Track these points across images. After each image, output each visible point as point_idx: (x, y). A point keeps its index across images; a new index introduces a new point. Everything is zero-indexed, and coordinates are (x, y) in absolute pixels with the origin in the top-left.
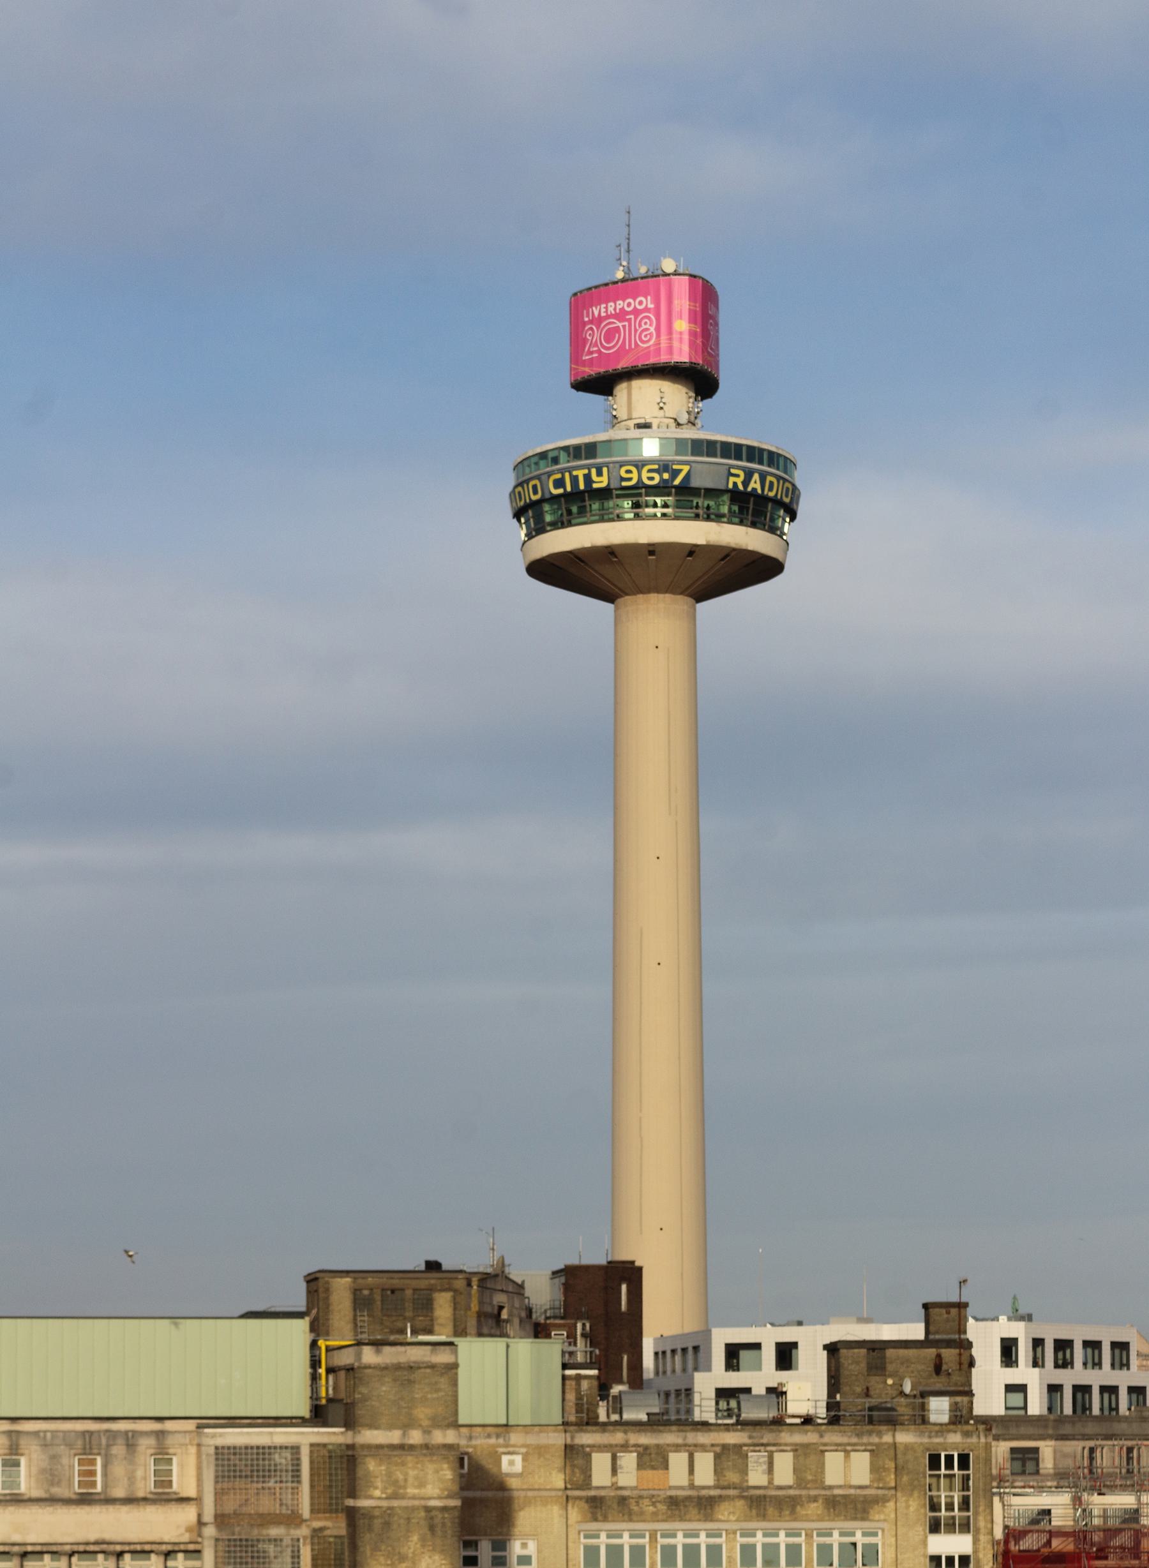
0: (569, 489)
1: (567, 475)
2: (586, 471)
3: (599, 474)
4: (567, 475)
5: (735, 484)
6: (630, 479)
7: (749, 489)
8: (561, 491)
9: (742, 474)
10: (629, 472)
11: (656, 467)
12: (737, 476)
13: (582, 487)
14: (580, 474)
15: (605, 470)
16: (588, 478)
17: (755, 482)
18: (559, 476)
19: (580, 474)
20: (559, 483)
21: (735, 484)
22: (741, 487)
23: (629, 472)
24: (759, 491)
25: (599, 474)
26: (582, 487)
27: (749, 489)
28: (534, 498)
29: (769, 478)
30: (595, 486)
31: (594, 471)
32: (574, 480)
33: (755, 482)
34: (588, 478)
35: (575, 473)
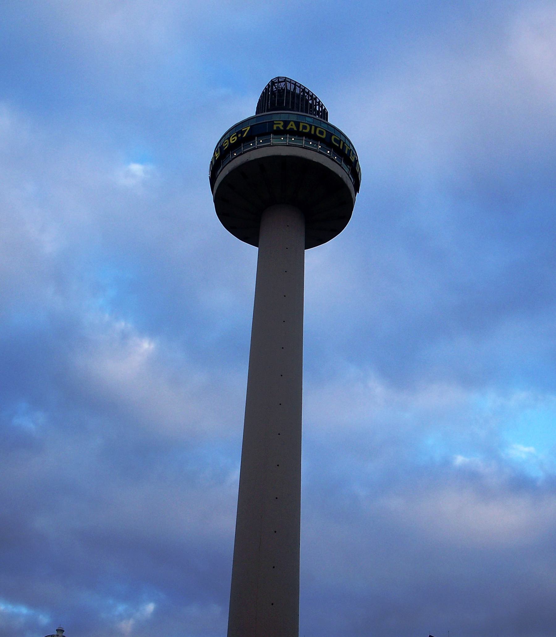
5: (277, 127)
7: (288, 128)
12: (280, 124)
17: (292, 125)
22: (282, 128)
24: (295, 129)
27: (288, 128)
29: (301, 125)
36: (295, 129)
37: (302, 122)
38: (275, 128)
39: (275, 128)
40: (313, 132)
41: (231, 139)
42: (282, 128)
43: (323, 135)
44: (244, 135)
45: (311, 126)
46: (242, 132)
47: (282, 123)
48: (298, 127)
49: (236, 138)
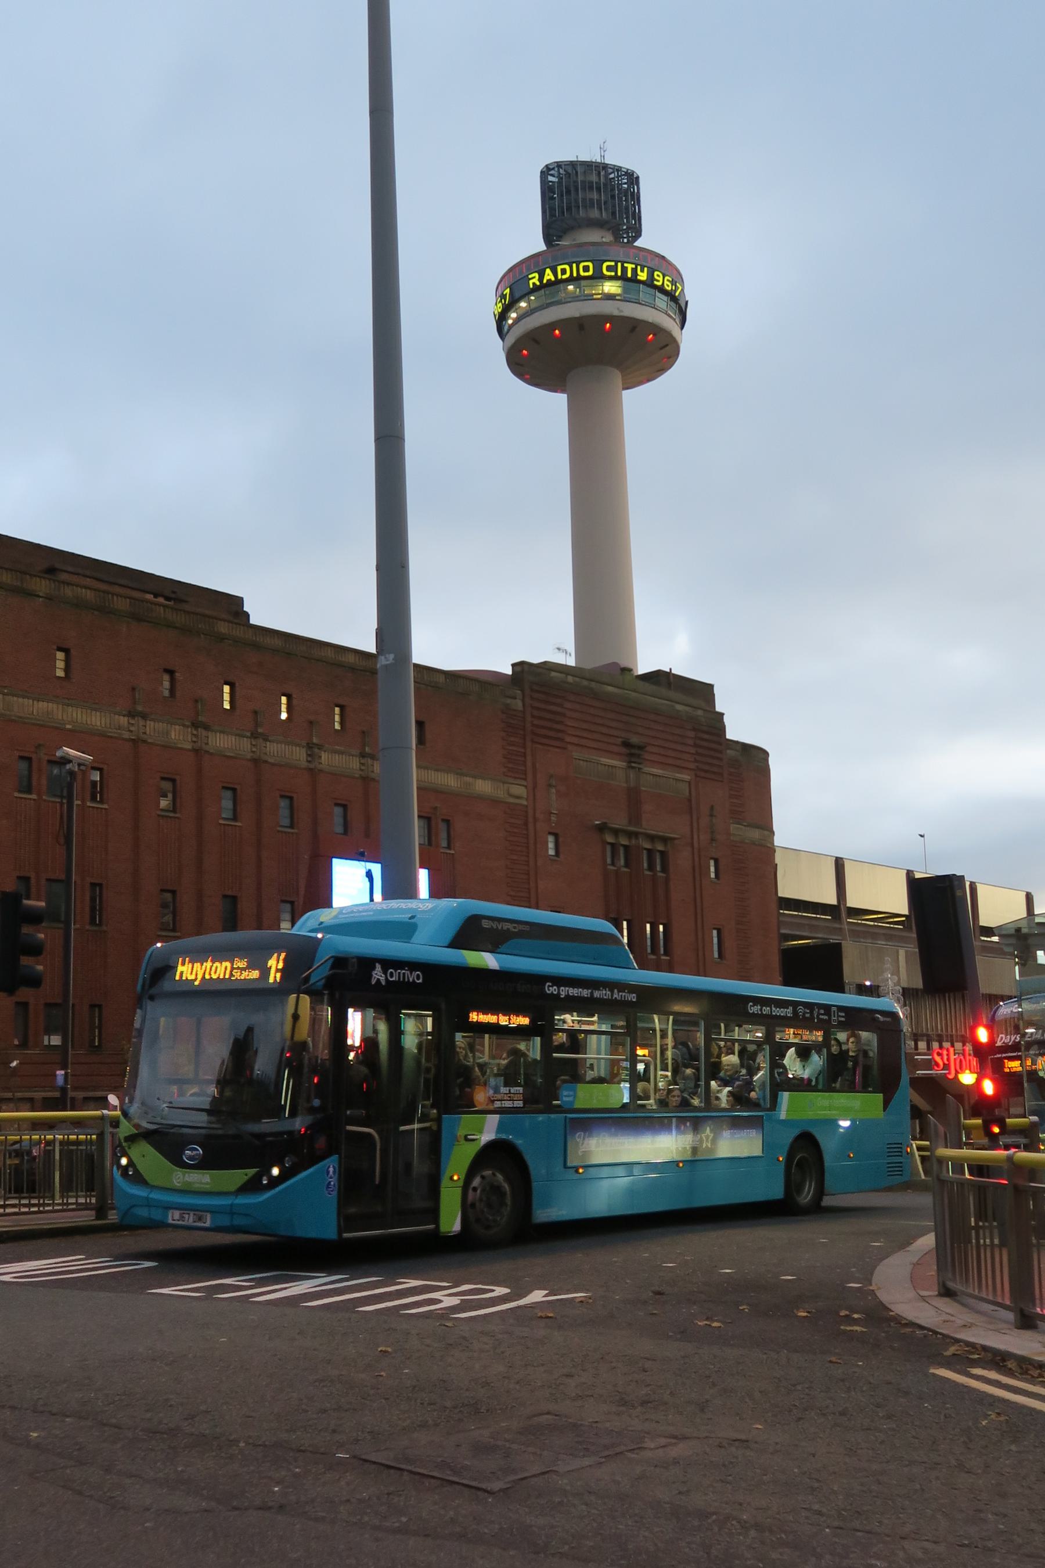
0: (619, 274)
1: (619, 265)
2: (634, 266)
3: (642, 271)
4: (619, 265)
6: (658, 281)
8: (613, 274)
10: (658, 276)
13: (629, 275)
14: (630, 267)
15: (646, 269)
16: (634, 271)
18: (613, 264)
19: (630, 267)
20: (609, 268)
23: (658, 276)
25: (642, 271)
26: (629, 275)
28: (582, 273)
31: (639, 268)
34: (634, 271)
35: (626, 265)
43: (588, 271)
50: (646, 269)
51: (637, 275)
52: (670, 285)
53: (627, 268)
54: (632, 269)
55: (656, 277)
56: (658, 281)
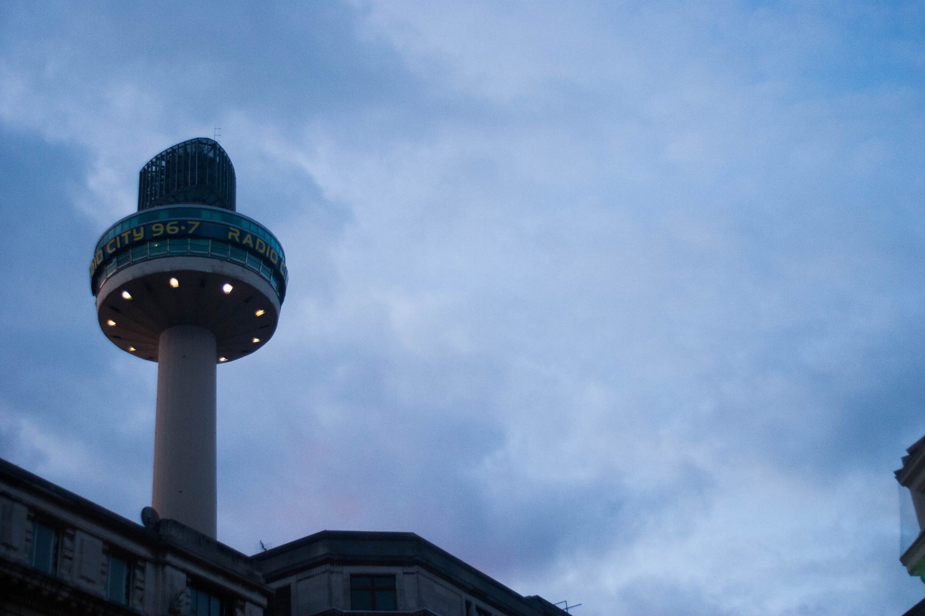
0: (119, 246)
2: (130, 232)
3: (138, 232)
5: (233, 237)
6: (159, 232)
7: (244, 242)
9: (238, 232)
10: (157, 227)
11: (176, 223)
12: (235, 232)
19: (126, 235)
21: (233, 237)
22: (237, 240)
23: (157, 227)
24: (252, 245)
25: (138, 232)
26: (127, 242)
27: (244, 242)
29: (258, 241)
30: (135, 239)
31: (135, 231)
32: (122, 239)
33: (249, 239)
34: (131, 236)
35: (123, 235)
36: (252, 245)
37: (259, 238)
38: (230, 237)
39: (230, 237)
40: (267, 255)
41: (168, 228)
42: (237, 240)
44: (191, 232)
45: (267, 245)
46: (189, 227)
47: (238, 234)
48: (254, 243)
49: (177, 229)
50: (142, 229)
51: (133, 237)
52: (177, 229)
53: (124, 237)
54: (129, 235)
55: (154, 228)
56: (159, 232)
